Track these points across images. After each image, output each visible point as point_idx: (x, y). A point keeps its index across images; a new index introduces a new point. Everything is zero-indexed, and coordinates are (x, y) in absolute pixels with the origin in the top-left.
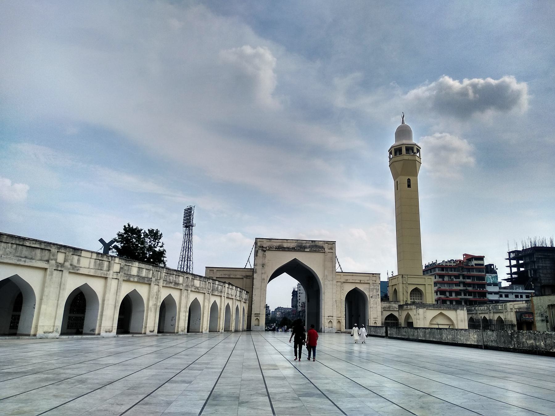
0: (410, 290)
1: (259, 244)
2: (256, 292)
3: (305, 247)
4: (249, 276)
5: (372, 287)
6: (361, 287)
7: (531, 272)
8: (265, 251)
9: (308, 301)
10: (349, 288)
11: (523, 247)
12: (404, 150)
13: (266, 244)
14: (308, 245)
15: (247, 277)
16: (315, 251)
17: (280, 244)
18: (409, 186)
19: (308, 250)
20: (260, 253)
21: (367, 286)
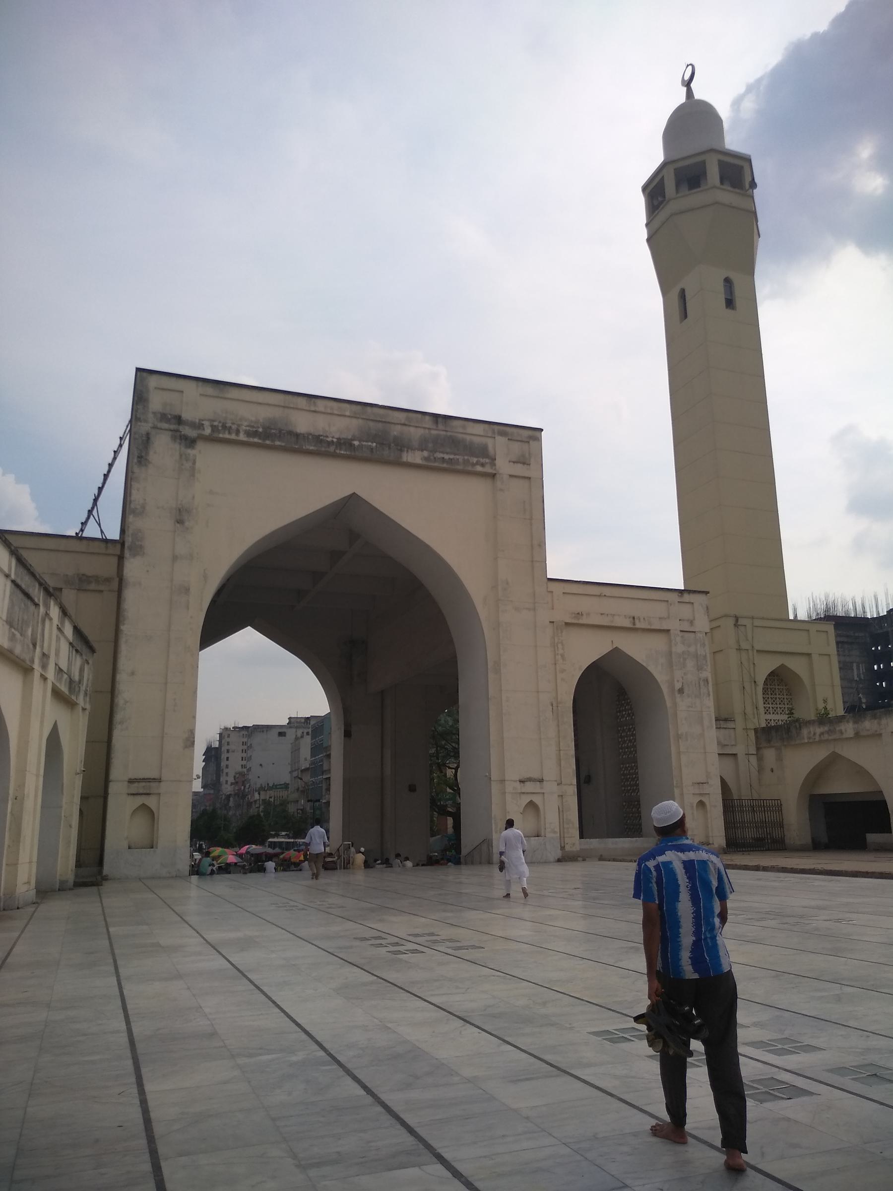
0: (761, 678)
1: (156, 402)
2: (137, 663)
3: (401, 445)
4: (97, 579)
5: (679, 648)
6: (638, 649)
7: (858, 669)
8: (191, 442)
9: (347, 734)
10: (587, 650)
11: (827, 609)
12: (713, 173)
13: (198, 408)
14: (415, 433)
15: (82, 582)
16: (449, 469)
17: (276, 413)
18: (730, 303)
19: (416, 457)
20: (164, 448)
21: (657, 643)
